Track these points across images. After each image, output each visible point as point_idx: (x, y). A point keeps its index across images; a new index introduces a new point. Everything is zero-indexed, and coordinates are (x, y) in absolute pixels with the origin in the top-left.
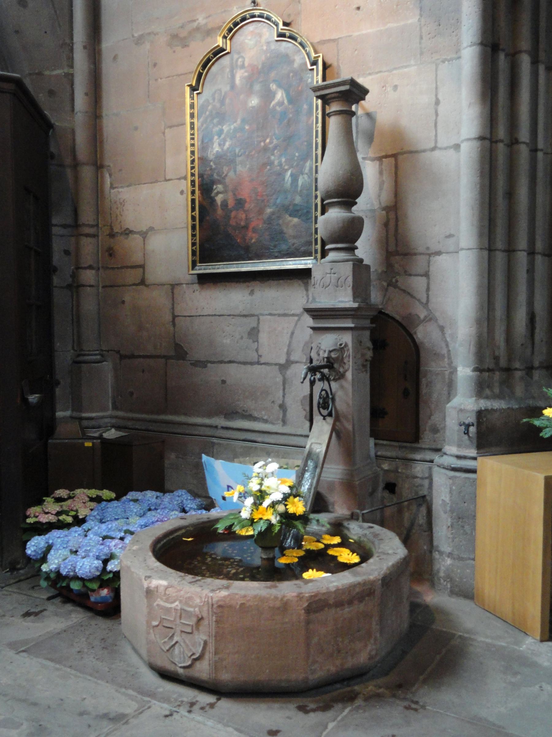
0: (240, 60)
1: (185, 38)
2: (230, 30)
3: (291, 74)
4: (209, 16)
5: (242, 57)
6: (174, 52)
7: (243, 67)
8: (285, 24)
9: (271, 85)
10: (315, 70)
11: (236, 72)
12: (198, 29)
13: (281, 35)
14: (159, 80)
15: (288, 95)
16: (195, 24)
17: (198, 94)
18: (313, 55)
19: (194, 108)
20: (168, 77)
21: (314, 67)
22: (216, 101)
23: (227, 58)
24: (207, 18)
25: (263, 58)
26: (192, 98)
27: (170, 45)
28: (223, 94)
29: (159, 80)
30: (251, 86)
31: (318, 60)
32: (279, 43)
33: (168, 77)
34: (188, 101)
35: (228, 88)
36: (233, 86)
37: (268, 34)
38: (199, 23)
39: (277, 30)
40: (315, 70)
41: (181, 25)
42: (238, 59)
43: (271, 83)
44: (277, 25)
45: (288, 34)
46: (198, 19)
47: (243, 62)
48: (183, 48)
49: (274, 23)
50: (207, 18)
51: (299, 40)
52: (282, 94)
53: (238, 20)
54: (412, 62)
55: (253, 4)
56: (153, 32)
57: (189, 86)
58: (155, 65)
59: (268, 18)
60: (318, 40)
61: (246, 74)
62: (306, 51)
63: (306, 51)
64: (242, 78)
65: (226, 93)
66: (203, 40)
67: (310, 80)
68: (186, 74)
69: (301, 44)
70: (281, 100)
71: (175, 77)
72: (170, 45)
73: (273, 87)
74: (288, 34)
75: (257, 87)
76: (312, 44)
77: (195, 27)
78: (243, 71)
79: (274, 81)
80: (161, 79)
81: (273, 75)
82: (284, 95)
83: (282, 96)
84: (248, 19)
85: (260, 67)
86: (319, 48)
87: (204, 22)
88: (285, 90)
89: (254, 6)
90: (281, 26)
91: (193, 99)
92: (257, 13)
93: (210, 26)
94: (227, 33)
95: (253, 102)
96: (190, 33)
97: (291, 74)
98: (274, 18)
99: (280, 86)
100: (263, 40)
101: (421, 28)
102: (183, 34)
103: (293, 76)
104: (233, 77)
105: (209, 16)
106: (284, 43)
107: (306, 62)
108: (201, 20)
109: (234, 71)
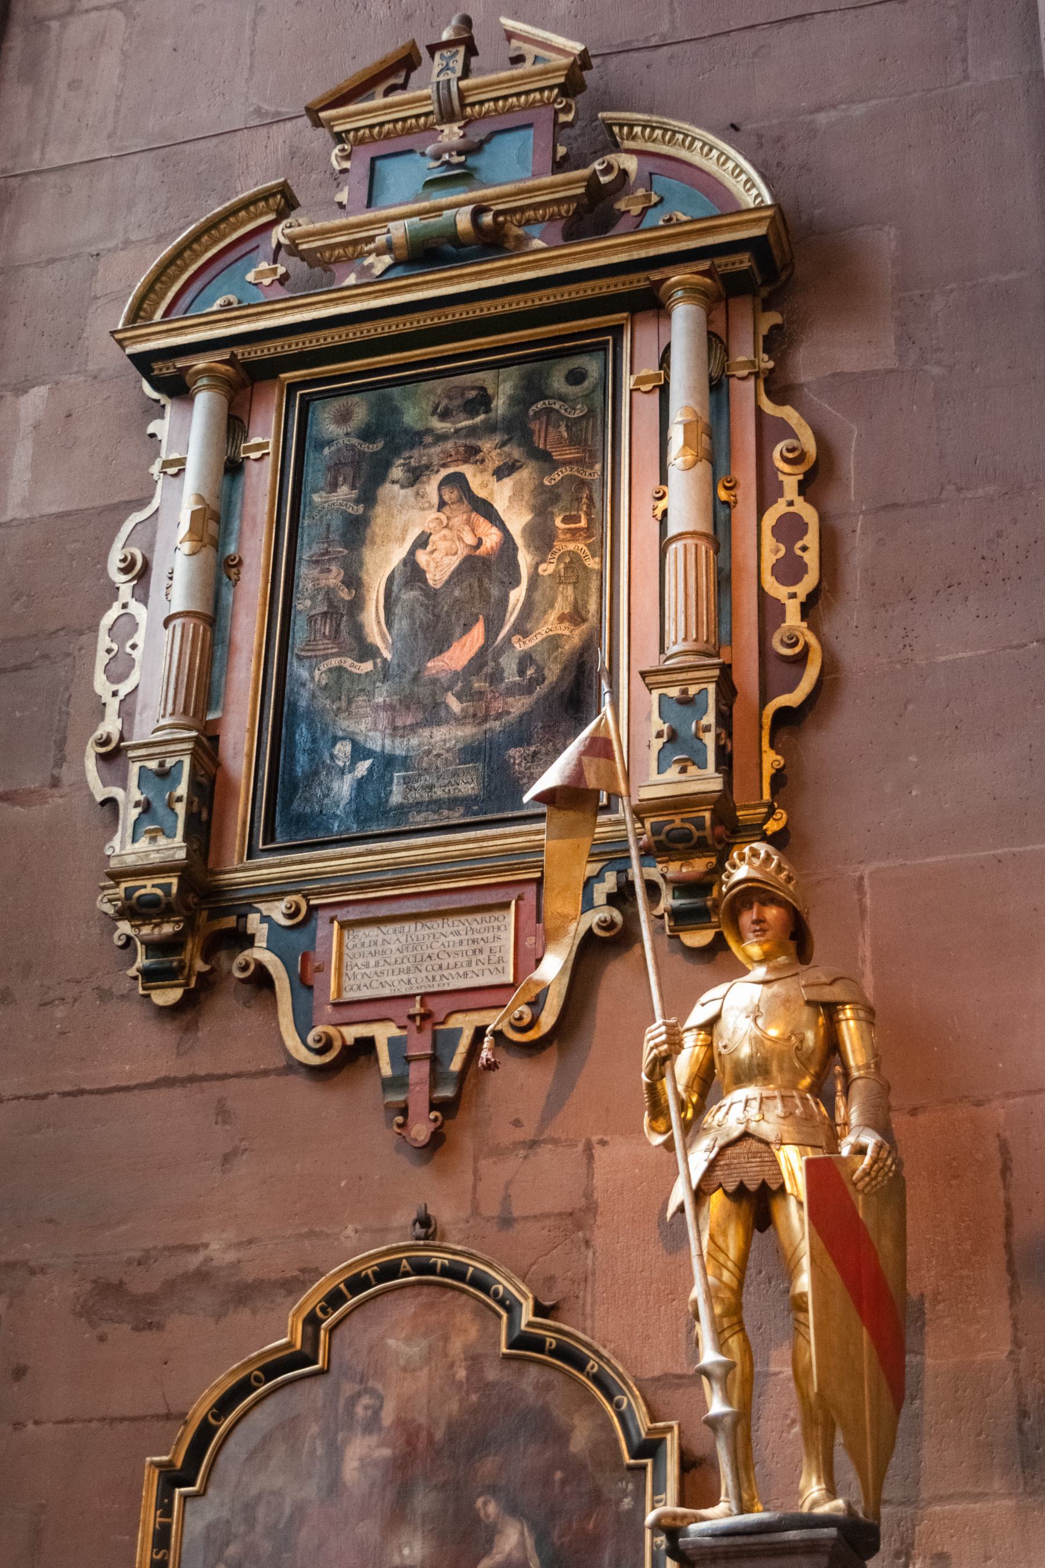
0: (366, 1400)
1: (151, 1299)
2: (334, 1299)
3: (558, 1475)
4: (250, 1242)
5: (372, 1392)
6: (102, 1339)
7: (372, 1424)
8: (540, 1310)
9: (480, 1502)
10: (649, 1469)
11: (346, 1442)
12: (202, 1276)
13: (523, 1342)
14: (31, 1426)
15: (541, 1539)
16: (194, 1261)
17: (185, 1497)
18: (643, 1422)
19: (167, 1547)
20: (68, 1421)
21: (649, 1462)
22: (259, 1528)
23: (318, 1390)
24: (240, 1245)
25: (453, 1407)
26: (165, 1508)
27: (86, 1312)
28: (287, 1510)
29: (31, 1426)
30: (403, 1495)
31: (663, 1440)
32: (515, 1365)
33: (68, 1421)
34: (149, 1518)
35: (311, 1490)
36: (334, 1486)
37: (473, 1333)
38: (209, 1259)
39: (512, 1323)
40: (649, 1469)
41: (138, 1254)
42: (359, 1395)
43: (479, 1495)
44: (512, 1308)
45: (551, 1342)
46: (206, 1246)
47: (377, 1412)
48: (136, 1329)
49: (501, 1302)
50: (240, 1245)
51: (593, 1366)
52: (522, 1534)
53: (369, 1269)
54: (996, 1485)
55: (419, 1231)
56: (25, 1263)
57: (159, 1465)
58: (19, 1373)
59: (482, 1283)
60: (657, 1373)
61: (386, 1452)
62: (617, 1406)
63: (617, 1406)
64: (364, 1464)
65: (300, 1510)
66: (219, 1316)
67: (627, 1503)
68: (143, 1418)
69: (598, 1379)
70: (517, 1555)
71: (94, 1425)
72: (86, 1312)
73: (490, 1509)
74: (551, 1342)
75: (424, 1501)
76: (638, 1381)
77: (192, 1267)
78: (373, 1440)
79: (492, 1490)
80: (36, 1423)
81: (489, 1465)
82: (530, 1543)
83: (522, 1544)
84: (406, 1274)
85: (439, 1435)
86: (662, 1397)
87: (231, 1256)
88: (534, 1527)
89: (426, 1237)
90: (527, 1315)
91: (167, 1512)
92: (441, 1259)
93: (250, 1274)
94: (323, 1310)
95: (406, 1551)
96: (170, 1286)
97: (558, 1475)
98: (503, 1284)
99: (513, 1509)
100: (456, 1346)
101: (1018, 1382)
102: (140, 1284)
103: (564, 1482)
104: (335, 1453)
105: (250, 1242)
106: (533, 1371)
107: (616, 1441)
108: (218, 1248)
109: (340, 1436)
